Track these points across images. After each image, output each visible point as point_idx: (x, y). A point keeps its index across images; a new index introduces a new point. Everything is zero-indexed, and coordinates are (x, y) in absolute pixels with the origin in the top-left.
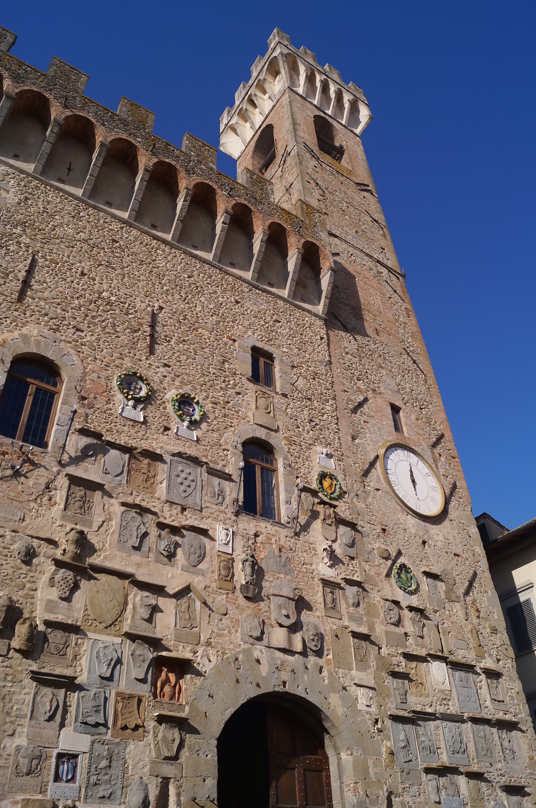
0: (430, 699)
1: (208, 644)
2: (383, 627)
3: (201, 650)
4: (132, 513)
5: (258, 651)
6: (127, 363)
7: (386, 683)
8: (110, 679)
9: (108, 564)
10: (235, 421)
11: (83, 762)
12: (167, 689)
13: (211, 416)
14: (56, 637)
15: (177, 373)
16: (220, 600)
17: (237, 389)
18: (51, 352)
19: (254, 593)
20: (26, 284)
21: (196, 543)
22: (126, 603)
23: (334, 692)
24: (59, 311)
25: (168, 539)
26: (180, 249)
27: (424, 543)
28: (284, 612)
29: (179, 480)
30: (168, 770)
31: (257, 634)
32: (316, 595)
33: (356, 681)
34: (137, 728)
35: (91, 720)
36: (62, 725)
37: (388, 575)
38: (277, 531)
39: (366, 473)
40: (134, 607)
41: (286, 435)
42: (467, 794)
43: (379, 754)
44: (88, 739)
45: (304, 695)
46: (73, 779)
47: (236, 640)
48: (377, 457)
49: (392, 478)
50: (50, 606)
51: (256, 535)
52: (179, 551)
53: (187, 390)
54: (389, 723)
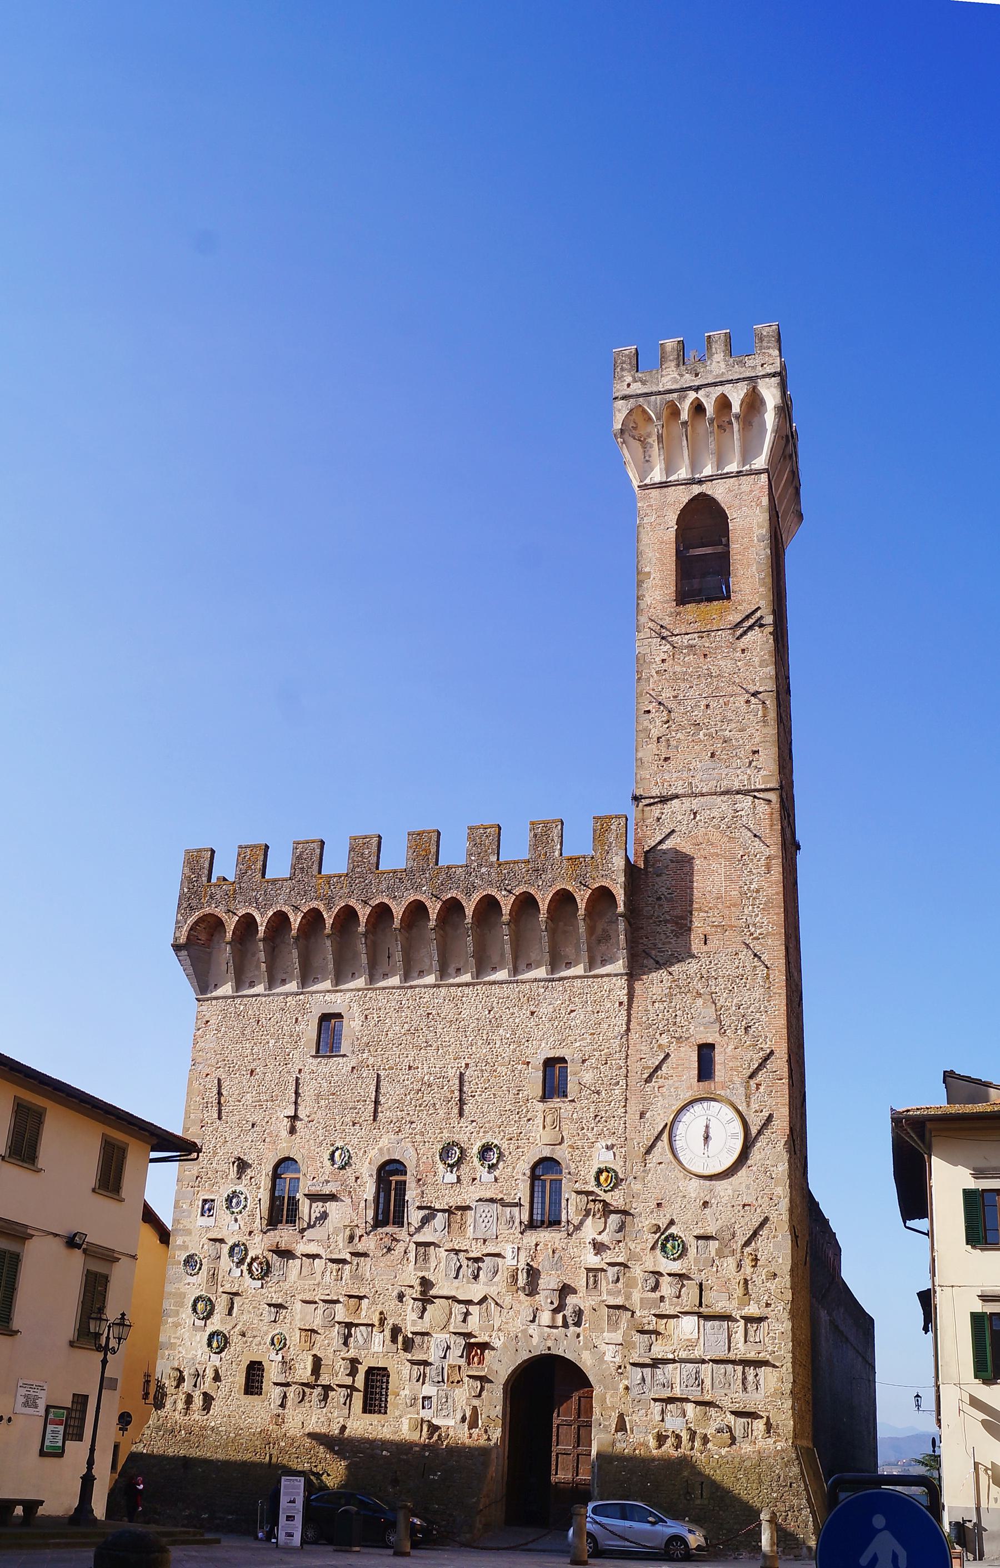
1: (499, 1330)
2: (639, 1295)
3: (494, 1334)
4: (452, 1255)
6: (446, 1134)
8: (445, 1357)
9: (441, 1293)
10: (525, 1150)
11: (434, 1400)
12: (476, 1359)
13: (506, 1153)
14: (418, 1339)
16: (507, 1300)
20: (377, 1102)
21: (491, 1265)
22: (451, 1313)
24: (399, 1113)
26: (480, 983)
27: (705, 1204)
28: (549, 1301)
30: (476, 1402)
32: (580, 1282)
34: (458, 1382)
35: (436, 1380)
36: (423, 1383)
37: (653, 1248)
39: (648, 1151)
42: (692, 1416)
47: (518, 1323)
49: (678, 1144)
50: (414, 1323)
51: (537, 1245)
52: (481, 1272)
53: (489, 1138)
54: (628, 1366)
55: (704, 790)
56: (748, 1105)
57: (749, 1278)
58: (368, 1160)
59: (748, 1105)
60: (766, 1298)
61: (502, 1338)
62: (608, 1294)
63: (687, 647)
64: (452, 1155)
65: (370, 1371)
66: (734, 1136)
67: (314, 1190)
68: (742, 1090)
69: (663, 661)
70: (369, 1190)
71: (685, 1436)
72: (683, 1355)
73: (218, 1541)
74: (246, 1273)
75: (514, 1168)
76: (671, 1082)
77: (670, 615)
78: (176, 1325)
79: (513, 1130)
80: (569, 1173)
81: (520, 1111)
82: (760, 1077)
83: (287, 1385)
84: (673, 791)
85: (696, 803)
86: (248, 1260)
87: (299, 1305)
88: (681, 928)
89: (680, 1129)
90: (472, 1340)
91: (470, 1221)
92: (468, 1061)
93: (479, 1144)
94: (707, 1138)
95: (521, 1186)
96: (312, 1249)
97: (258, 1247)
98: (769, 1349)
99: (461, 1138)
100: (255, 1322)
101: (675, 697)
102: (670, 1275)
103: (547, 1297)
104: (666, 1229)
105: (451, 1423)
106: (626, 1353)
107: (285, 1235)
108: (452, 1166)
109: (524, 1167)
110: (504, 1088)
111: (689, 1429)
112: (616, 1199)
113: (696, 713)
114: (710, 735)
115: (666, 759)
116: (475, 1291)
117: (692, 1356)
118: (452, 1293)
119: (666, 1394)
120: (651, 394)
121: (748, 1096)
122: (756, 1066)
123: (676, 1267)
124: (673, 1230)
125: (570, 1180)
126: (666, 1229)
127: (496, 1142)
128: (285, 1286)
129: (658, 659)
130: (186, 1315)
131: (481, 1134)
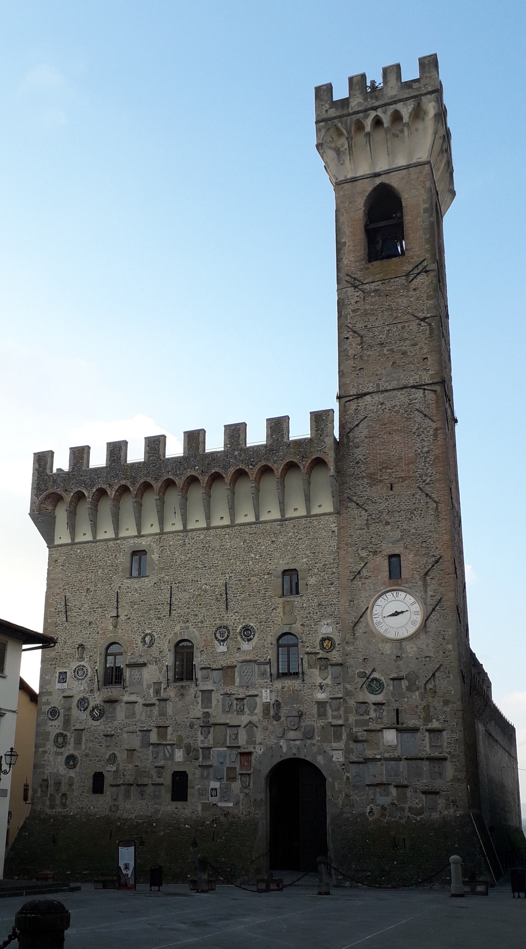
1: (261, 744)
3: (257, 747)
5: (282, 742)
10: (272, 629)
11: (218, 791)
28: (293, 723)
29: (244, 674)
31: (281, 735)
38: (293, 683)
40: (230, 736)
44: (219, 783)
45: (304, 758)
46: (216, 796)
50: (202, 742)
55: (388, 388)
58: (168, 640)
61: (262, 749)
63: (374, 291)
64: (223, 633)
65: (176, 774)
67: (132, 661)
70: (169, 659)
73: (78, 889)
74: (89, 717)
76: (369, 581)
77: (361, 270)
78: (45, 752)
80: (302, 642)
83: (118, 786)
86: (90, 708)
87: (125, 735)
88: (373, 481)
90: (243, 750)
91: (237, 675)
93: (241, 626)
95: (270, 652)
96: (133, 698)
97: (96, 699)
99: (229, 623)
100: (97, 747)
103: (291, 722)
105: (231, 805)
107: (114, 691)
113: (381, 336)
114: (392, 350)
115: (360, 369)
118: (228, 721)
125: (303, 646)
128: (116, 723)
129: (353, 301)
130: (50, 746)
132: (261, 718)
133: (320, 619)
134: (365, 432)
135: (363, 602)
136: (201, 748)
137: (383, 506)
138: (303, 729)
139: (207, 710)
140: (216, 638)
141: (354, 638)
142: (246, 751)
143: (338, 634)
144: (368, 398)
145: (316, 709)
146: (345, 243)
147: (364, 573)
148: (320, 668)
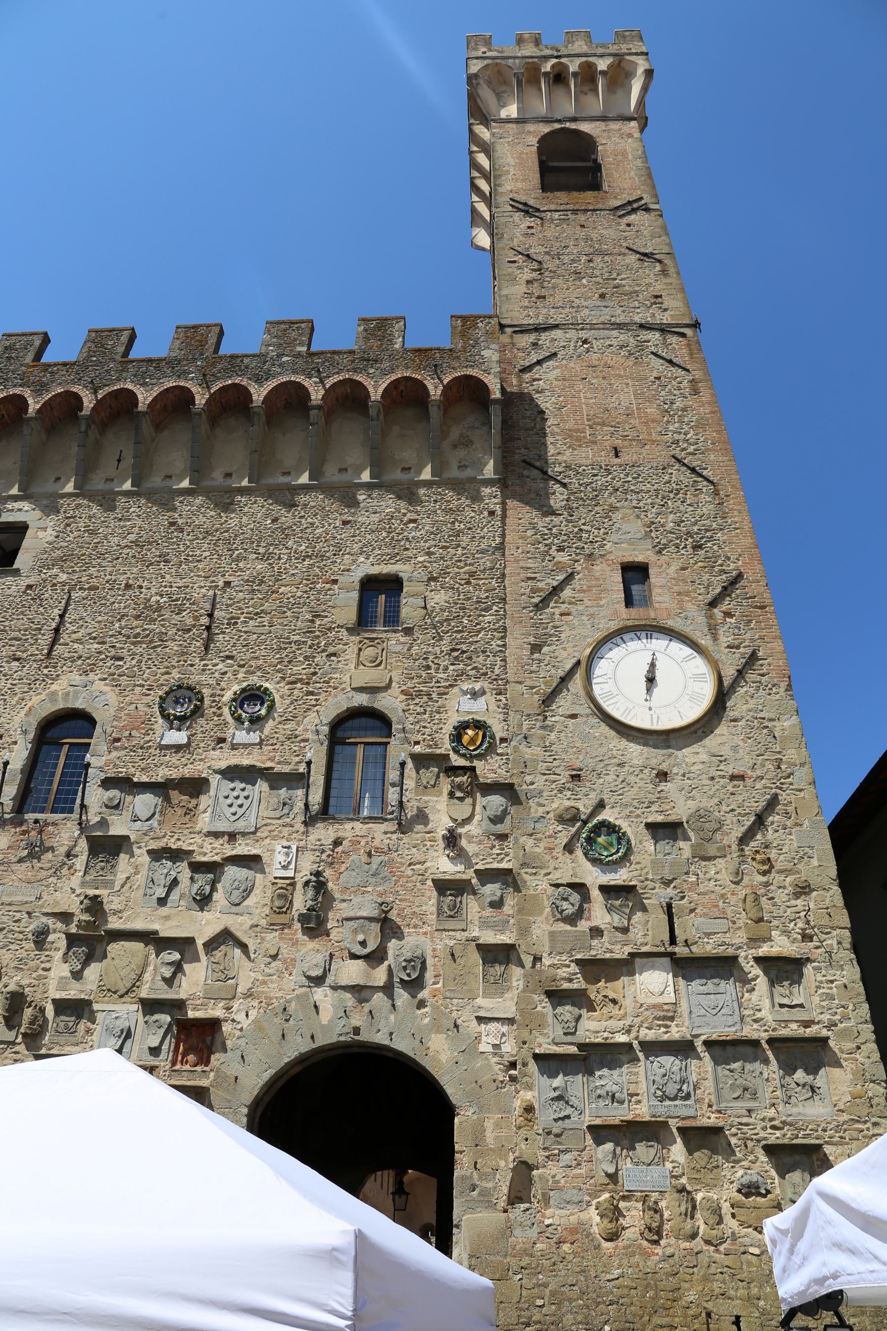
0: (628, 1022)
1: (249, 995)
5: (320, 994)
6: (175, 674)
7: (539, 1008)
10: (322, 697)
15: (242, 663)
17: (331, 649)
18: (80, 701)
19: (314, 924)
23: (438, 1031)
25: (203, 880)
27: (663, 776)
28: (361, 937)
31: (316, 972)
33: (482, 1014)
41: (404, 688)
43: (507, 1110)
45: (386, 1042)
47: (287, 986)
48: (578, 663)
53: (255, 680)
54: (533, 1067)
56: (715, 638)
57: (762, 891)
59: (715, 638)
60: (801, 925)
61: (253, 1014)
62: (479, 923)
64: (183, 704)
66: (698, 677)
68: (701, 619)
69: (529, 227)
71: (669, 1206)
72: (649, 1035)
75: (298, 724)
76: (581, 608)
79: (299, 669)
81: (317, 639)
82: (724, 606)
84: (551, 321)
85: (583, 334)
89: (602, 668)
92: (231, 579)
93: (236, 688)
94: (651, 680)
98: (826, 1017)
101: (547, 253)
102: (606, 890)
103: (355, 932)
104: (592, 815)
106: (525, 1035)
108: (182, 719)
109: (316, 722)
110: (289, 614)
111: (682, 1190)
112: (489, 770)
116: (203, 926)
117: (666, 1037)
119: (618, 1114)
120: (510, 58)
121: (713, 630)
122: (719, 590)
123: (621, 877)
124: (607, 815)
126: (592, 815)
127: (267, 685)
131: (241, 676)
132: (263, 922)
133: (456, 680)
134: (557, 372)
135: (564, 649)
136: (54, 1001)
137: (601, 481)
138: (391, 960)
139: (97, 892)
140: (162, 710)
141: (542, 727)
142: (199, 1014)
143: (501, 716)
144: (557, 334)
145: (434, 901)
146: (508, 172)
147: (567, 593)
148: (451, 795)
